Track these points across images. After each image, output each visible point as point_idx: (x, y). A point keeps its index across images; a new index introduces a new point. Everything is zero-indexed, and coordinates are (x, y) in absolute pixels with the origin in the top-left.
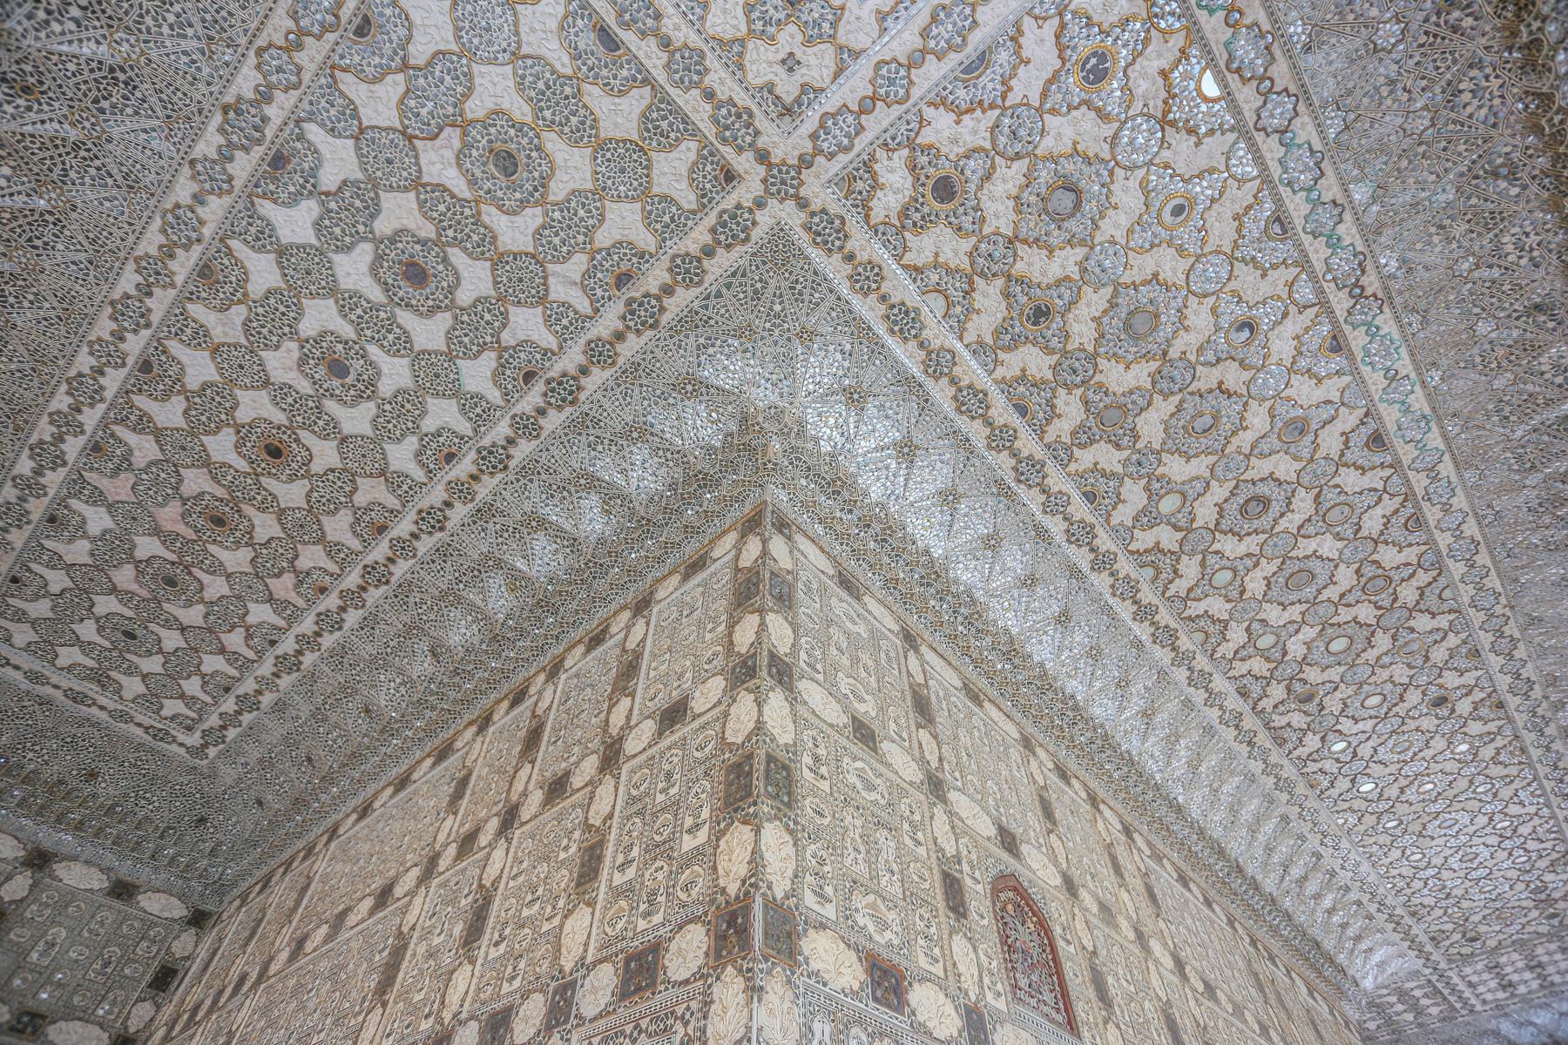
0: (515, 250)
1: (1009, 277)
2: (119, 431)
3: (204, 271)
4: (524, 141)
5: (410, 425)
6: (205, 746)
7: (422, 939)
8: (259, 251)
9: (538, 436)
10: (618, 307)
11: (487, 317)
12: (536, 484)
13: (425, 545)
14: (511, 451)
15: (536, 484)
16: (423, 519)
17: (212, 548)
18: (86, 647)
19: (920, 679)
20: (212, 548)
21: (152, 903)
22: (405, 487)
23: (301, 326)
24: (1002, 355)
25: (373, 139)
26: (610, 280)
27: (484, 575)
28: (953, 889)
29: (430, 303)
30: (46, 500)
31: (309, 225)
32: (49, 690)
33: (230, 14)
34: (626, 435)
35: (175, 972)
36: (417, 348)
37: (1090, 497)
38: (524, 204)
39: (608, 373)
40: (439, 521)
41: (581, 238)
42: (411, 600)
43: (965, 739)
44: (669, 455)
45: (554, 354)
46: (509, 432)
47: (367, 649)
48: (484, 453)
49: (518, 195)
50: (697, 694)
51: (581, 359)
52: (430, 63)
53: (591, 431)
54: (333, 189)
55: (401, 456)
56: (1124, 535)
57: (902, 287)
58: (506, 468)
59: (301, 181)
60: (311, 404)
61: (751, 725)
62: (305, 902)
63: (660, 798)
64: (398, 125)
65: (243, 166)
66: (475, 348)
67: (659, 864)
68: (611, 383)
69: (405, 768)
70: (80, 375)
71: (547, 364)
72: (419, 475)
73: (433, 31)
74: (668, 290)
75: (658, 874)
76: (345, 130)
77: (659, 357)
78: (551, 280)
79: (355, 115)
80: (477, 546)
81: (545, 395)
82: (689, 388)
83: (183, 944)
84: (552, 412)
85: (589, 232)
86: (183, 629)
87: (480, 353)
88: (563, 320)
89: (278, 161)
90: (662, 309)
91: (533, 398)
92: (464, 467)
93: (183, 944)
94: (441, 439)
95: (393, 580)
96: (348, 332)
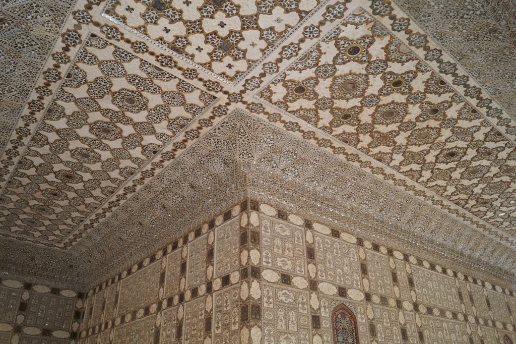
1: (331, 108)
4: (135, 95)
7: (164, 330)
8: (50, 132)
12: (165, 179)
15: (165, 179)
18: (19, 226)
19: (311, 241)
21: (65, 293)
24: (333, 129)
28: (316, 321)
35: (80, 313)
37: (380, 160)
43: (329, 256)
47: (116, 223)
50: (232, 276)
56: (398, 168)
57: (287, 118)
61: (247, 296)
63: (225, 309)
67: (227, 331)
68: (185, 153)
71: (161, 149)
75: (226, 334)
78: (155, 128)
83: (79, 304)
87: (135, 148)
92: (138, 176)
93: (79, 304)
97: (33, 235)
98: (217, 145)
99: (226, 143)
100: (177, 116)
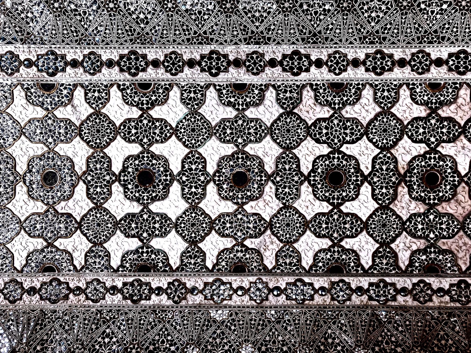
0: (85, 144)
5: (240, 122)
10: (60, 78)
12: (204, 28)
15: (204, 28)
23: (231, 210)
25: (95, 238)
26: (54, 92)
29: (154, 162)
33: (85, 319)
36: (187, 151)
39: (100, 52)
42: (377, 27)
45: (119, 86)
51: (105, 70)
53: (138, 30)
64: (78, 231)
66: (157, 124)
74: (30, 64)
78: (84, 118)
84: (150, 57)
88: (98, 96)
89: (145, 268)
94: (232, 100)
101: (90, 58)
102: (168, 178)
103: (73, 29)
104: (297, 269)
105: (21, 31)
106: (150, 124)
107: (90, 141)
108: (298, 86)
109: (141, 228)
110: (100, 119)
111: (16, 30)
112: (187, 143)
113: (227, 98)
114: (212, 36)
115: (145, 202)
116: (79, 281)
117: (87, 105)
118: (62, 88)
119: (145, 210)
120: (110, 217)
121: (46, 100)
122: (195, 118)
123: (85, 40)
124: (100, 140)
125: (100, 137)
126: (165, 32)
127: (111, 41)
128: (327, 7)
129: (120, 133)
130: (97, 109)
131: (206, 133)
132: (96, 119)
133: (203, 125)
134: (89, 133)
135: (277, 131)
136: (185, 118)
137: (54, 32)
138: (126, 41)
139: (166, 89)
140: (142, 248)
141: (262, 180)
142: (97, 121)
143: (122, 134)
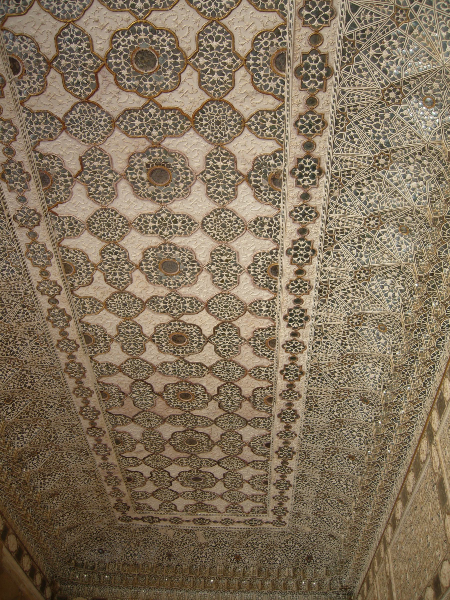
0: (198, 107)
2: (105, 380)
3: (67, 268)
5: (235, 268)
6: (279, 517)
9: (317, 215)
11: (220, 164)
13: (306, 335)
14: (309, 238)
15: (342, 247)
16: (291, 321)
17: (195, 412)
20: (195, 412)
22: (264, 309)
27: (357, 331)
29: (182, 185)
30: (107, 435)
31: (87, 200)
32: (185, 525)
34: (377, 167)
38: (177, 76)
40: (301, 315)
41: (229, 61)
44: (418, 157)
45: (280, 151)
46: (297, 226)
48: (293, 252)
49: (169, 72)
51: (301, 140)
52: (59, 48)
53: (349, 183)
54: (79, 168)
55: (247, 291)
58: (314, 251)
59: (62, 179)
60: (174, 298)
62: (394, 594)
65: (35, 199)
66: (230, 190)
69: (400, 485)
70: (67, 365)
72: (265, 295)
73: (43, 29)
74: (316, 39)
76: (55, 130)
77: (352, 91)
78: (236, 106)
79: (53, 117)
80: (336, 315)
81: (298, 183)
82: (392, 95)
85: (231, 50)
86: (218, 463)
89: (45, 179)
90: (324, 57)
91: (291, 194)
92: (288, 271)
94: (260, 263)
95: (304, 369)
96: (155, 241)
97: (215, 509)
98: (383, 64)
99: (396, 43)
100: (251, 37)
101: (318, 121)
102: (162, 200)
103: (359, 108)
104: (81, 313)
105: (363, 36)
106: (230, 183)
107: (203, 113)
108: (273, 316)
109: (95, 173)
110: (235, 126)
111: (365, 30)
112: (208, 219)
113: (262, 259)
114: (332, 254)
115: (129, 176)
116: (10, 111)
117: (254, 112)
118: (278, 81)
119: (118, 176)
120: (103, 138)
121: (261, 58)
122: (239, 228)
123: (342, 120)
124: (206, 125)
125: (211, 125)
126: (342, 211)
127: (338, 152)
128: (348, 347)
129: (217, 148)
130: (249, 123)
131: (221, 237)
132: (235, 120)
133: (230, 235)
134: (215, 111)
135: (225, 298)
136: (238, 218)
137: (357, 83)
138: (336, 168)
139: (274, 203)
140: (70, 175)
141: (170, 285)
142: (232, 123)
143: (215, 151)
